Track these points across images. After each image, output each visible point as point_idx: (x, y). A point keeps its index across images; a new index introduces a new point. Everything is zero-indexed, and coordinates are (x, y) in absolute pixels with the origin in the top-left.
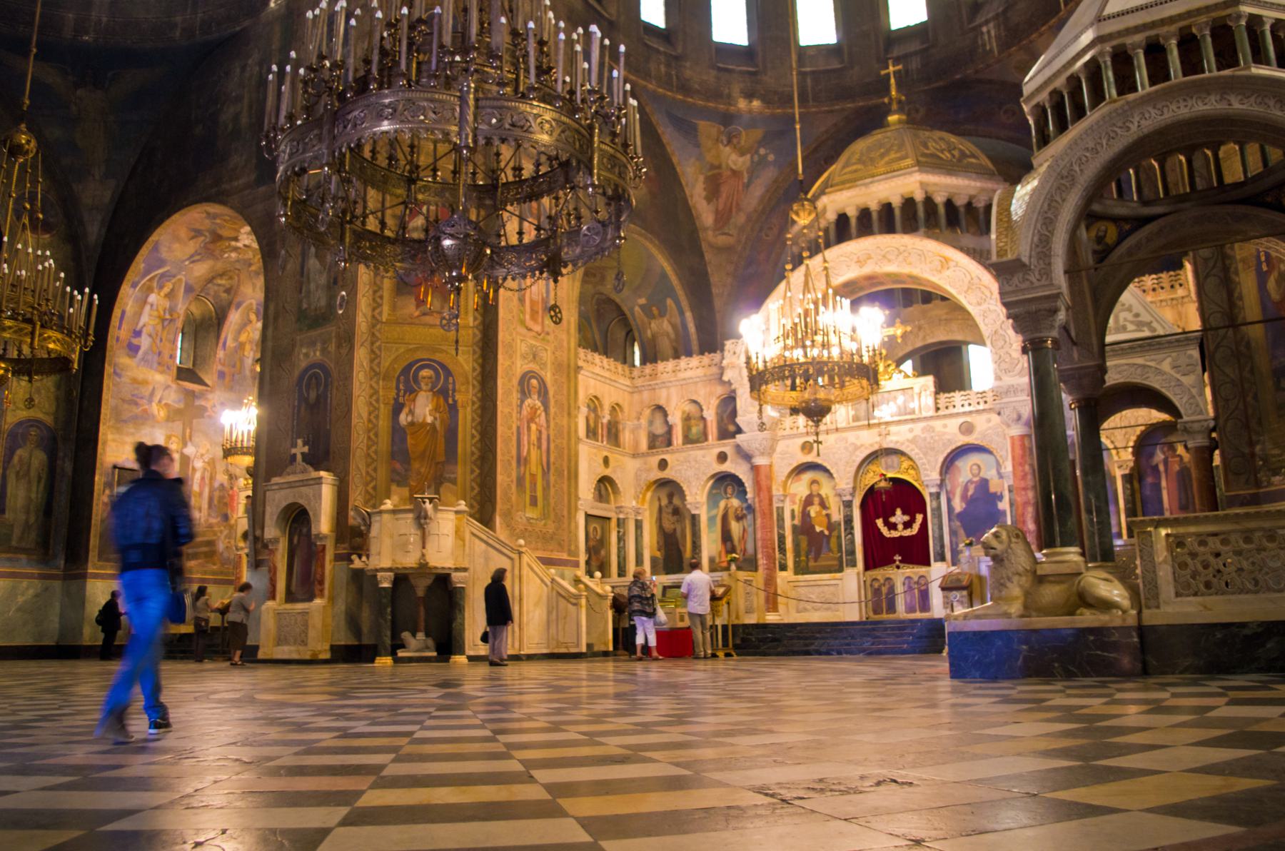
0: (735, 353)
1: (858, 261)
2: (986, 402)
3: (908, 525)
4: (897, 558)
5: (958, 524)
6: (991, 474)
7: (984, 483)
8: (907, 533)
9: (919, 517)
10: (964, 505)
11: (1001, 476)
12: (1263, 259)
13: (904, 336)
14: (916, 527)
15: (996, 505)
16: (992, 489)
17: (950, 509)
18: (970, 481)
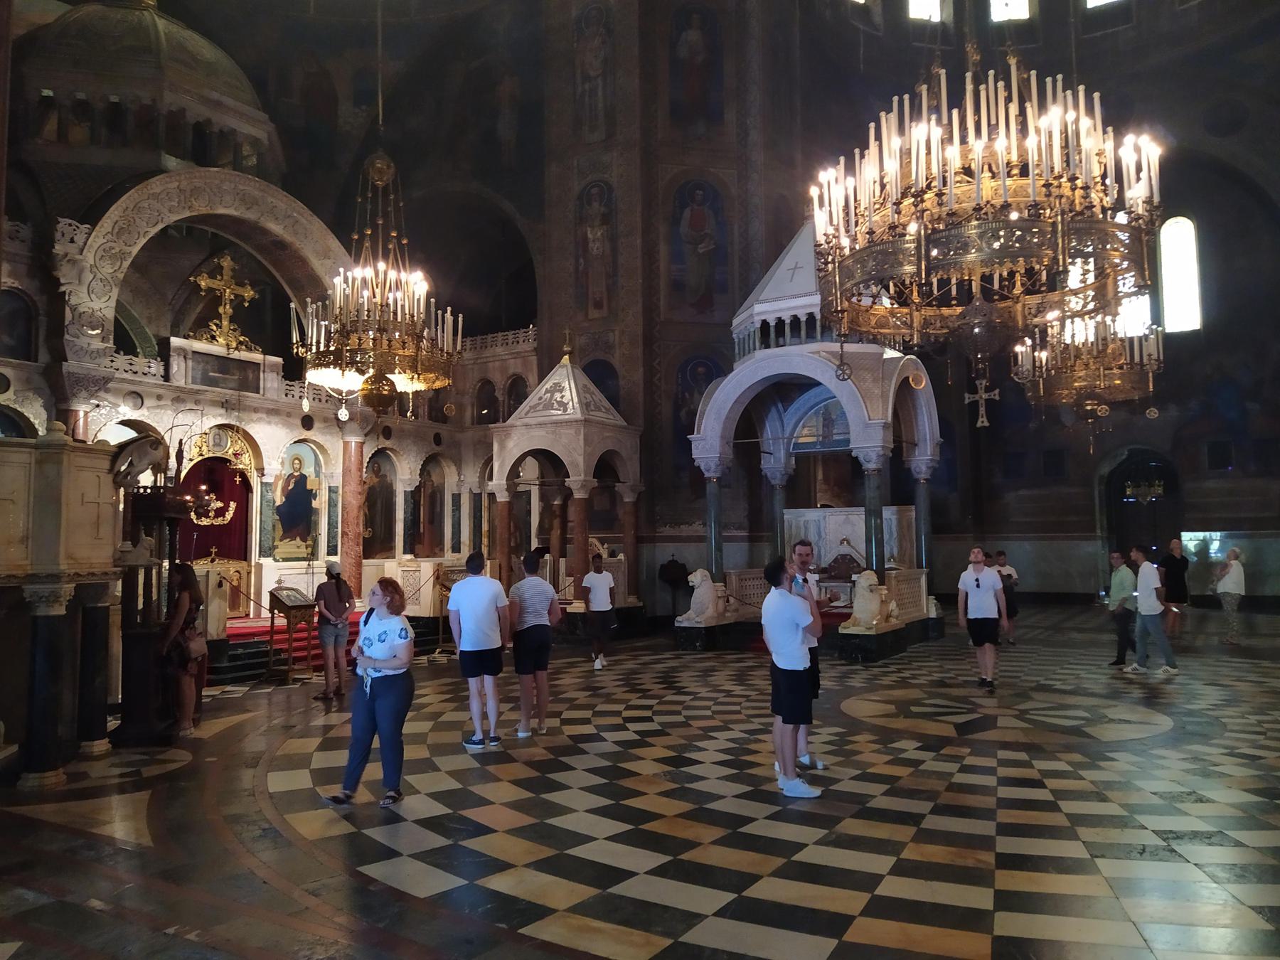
0: (72, 241)
1: (242, 200)
2: (320, 400)
3: (220, 512)
4: (214, 550)
5: (278, 517)
6: (309, 471)
7: (303, 478)
8: (219, 521)
9: (233, 505)
10: (284, 500)
11: (318, 474)
12: (680, 396)
13: (252, 301)
14: (229, 515)
15: (311, 503)
16: (309, 487)
17: (274, 502)
18: (291, 475)
